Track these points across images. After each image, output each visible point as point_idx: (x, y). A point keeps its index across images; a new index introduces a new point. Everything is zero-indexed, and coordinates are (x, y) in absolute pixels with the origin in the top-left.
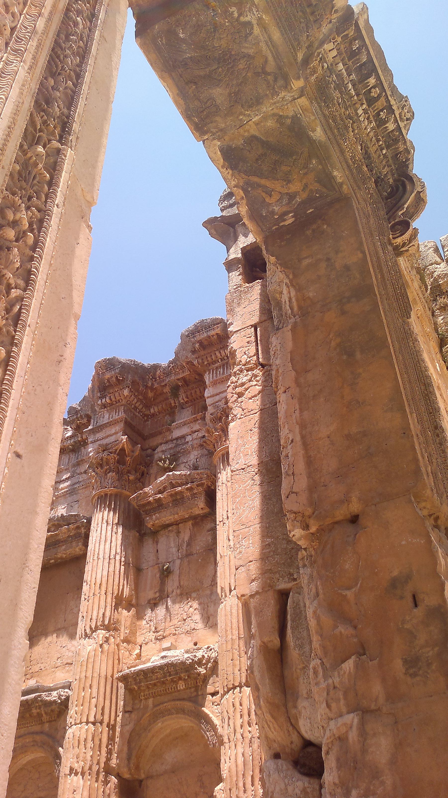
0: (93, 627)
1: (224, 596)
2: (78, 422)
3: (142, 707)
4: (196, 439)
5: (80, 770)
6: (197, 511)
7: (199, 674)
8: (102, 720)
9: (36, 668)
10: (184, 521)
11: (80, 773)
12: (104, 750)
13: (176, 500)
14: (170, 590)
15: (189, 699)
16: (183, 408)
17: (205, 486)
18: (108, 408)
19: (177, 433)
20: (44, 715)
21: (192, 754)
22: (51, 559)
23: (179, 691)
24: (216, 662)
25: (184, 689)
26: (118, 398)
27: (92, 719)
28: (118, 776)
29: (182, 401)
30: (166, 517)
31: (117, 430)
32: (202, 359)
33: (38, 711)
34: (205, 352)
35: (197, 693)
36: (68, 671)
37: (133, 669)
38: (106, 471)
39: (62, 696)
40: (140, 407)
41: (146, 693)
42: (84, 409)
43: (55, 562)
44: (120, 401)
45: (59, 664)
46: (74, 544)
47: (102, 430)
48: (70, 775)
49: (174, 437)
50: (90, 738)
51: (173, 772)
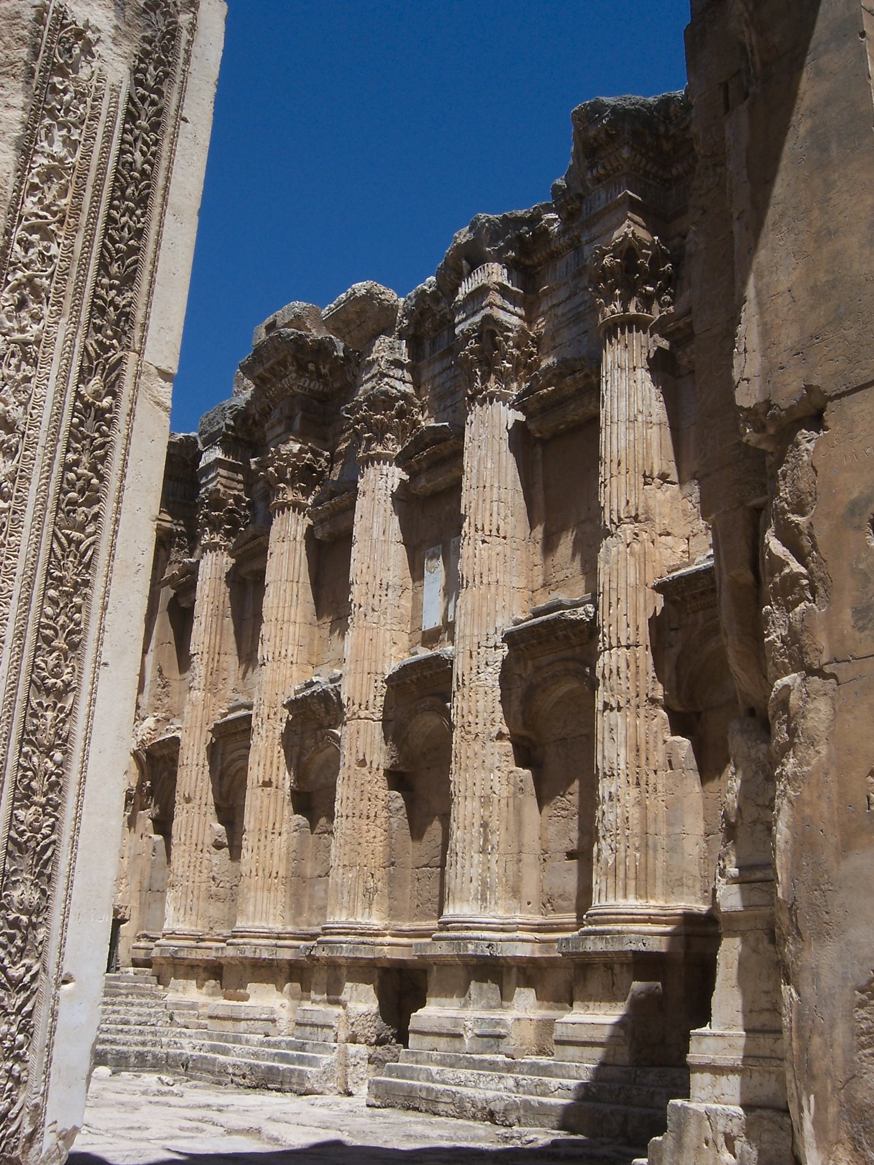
9: (560, 576)
20: (573, 637)
22: (560, 424)
28: (666, 708)
33: (565, 632)
37: (675, 574)
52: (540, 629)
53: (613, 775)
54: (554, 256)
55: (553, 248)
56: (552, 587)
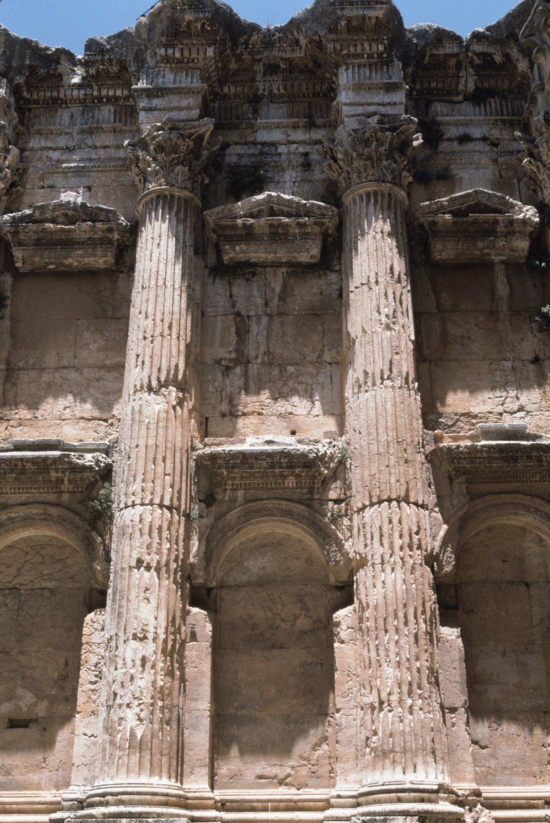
0: (163, 379)
1: (370, 384)
2: (101, 67)
3: (227, 498)
4: (294, 153)
5: (154, 564)
6: (303, 258)
7: (320, 474)
8: (180, 505)
10: (276, 265)
11: (153, 569)
12: (181, 544)
13: (276, 234)
14: (252, 354)
15: (300, 502)
16: (271, 102)
17: (325, 227)
18: (174, 65)
19: (263, 136)
21: (288, 569)
22: (52, 263)
23: (284, 488)
24: (342, 462)
25: (293, 488)
26: (194, 55)
27: (167, 502)
29: (276, 91)
30: (256, 253)
31: (191, 104)
32: (341, 46)
33: (60, 475)
34: (350, 37)
35: (312, 495)
36: (83, 429)
38: (172, 161)
39: (101, 462)
40: (214, 79)
41: (235, 482)
42: (116, 50)
43: (57, 268)
44: (196, 61)
46: (99, 252)
47: (163, 96)
48: (138, 567)
49: (259, 140)
50: (165, 526)
51: (261, 586)
52: (29, 465)
53: (145, 638)
54: (57, 103)
55: (62, 96)
56: (12, 423)
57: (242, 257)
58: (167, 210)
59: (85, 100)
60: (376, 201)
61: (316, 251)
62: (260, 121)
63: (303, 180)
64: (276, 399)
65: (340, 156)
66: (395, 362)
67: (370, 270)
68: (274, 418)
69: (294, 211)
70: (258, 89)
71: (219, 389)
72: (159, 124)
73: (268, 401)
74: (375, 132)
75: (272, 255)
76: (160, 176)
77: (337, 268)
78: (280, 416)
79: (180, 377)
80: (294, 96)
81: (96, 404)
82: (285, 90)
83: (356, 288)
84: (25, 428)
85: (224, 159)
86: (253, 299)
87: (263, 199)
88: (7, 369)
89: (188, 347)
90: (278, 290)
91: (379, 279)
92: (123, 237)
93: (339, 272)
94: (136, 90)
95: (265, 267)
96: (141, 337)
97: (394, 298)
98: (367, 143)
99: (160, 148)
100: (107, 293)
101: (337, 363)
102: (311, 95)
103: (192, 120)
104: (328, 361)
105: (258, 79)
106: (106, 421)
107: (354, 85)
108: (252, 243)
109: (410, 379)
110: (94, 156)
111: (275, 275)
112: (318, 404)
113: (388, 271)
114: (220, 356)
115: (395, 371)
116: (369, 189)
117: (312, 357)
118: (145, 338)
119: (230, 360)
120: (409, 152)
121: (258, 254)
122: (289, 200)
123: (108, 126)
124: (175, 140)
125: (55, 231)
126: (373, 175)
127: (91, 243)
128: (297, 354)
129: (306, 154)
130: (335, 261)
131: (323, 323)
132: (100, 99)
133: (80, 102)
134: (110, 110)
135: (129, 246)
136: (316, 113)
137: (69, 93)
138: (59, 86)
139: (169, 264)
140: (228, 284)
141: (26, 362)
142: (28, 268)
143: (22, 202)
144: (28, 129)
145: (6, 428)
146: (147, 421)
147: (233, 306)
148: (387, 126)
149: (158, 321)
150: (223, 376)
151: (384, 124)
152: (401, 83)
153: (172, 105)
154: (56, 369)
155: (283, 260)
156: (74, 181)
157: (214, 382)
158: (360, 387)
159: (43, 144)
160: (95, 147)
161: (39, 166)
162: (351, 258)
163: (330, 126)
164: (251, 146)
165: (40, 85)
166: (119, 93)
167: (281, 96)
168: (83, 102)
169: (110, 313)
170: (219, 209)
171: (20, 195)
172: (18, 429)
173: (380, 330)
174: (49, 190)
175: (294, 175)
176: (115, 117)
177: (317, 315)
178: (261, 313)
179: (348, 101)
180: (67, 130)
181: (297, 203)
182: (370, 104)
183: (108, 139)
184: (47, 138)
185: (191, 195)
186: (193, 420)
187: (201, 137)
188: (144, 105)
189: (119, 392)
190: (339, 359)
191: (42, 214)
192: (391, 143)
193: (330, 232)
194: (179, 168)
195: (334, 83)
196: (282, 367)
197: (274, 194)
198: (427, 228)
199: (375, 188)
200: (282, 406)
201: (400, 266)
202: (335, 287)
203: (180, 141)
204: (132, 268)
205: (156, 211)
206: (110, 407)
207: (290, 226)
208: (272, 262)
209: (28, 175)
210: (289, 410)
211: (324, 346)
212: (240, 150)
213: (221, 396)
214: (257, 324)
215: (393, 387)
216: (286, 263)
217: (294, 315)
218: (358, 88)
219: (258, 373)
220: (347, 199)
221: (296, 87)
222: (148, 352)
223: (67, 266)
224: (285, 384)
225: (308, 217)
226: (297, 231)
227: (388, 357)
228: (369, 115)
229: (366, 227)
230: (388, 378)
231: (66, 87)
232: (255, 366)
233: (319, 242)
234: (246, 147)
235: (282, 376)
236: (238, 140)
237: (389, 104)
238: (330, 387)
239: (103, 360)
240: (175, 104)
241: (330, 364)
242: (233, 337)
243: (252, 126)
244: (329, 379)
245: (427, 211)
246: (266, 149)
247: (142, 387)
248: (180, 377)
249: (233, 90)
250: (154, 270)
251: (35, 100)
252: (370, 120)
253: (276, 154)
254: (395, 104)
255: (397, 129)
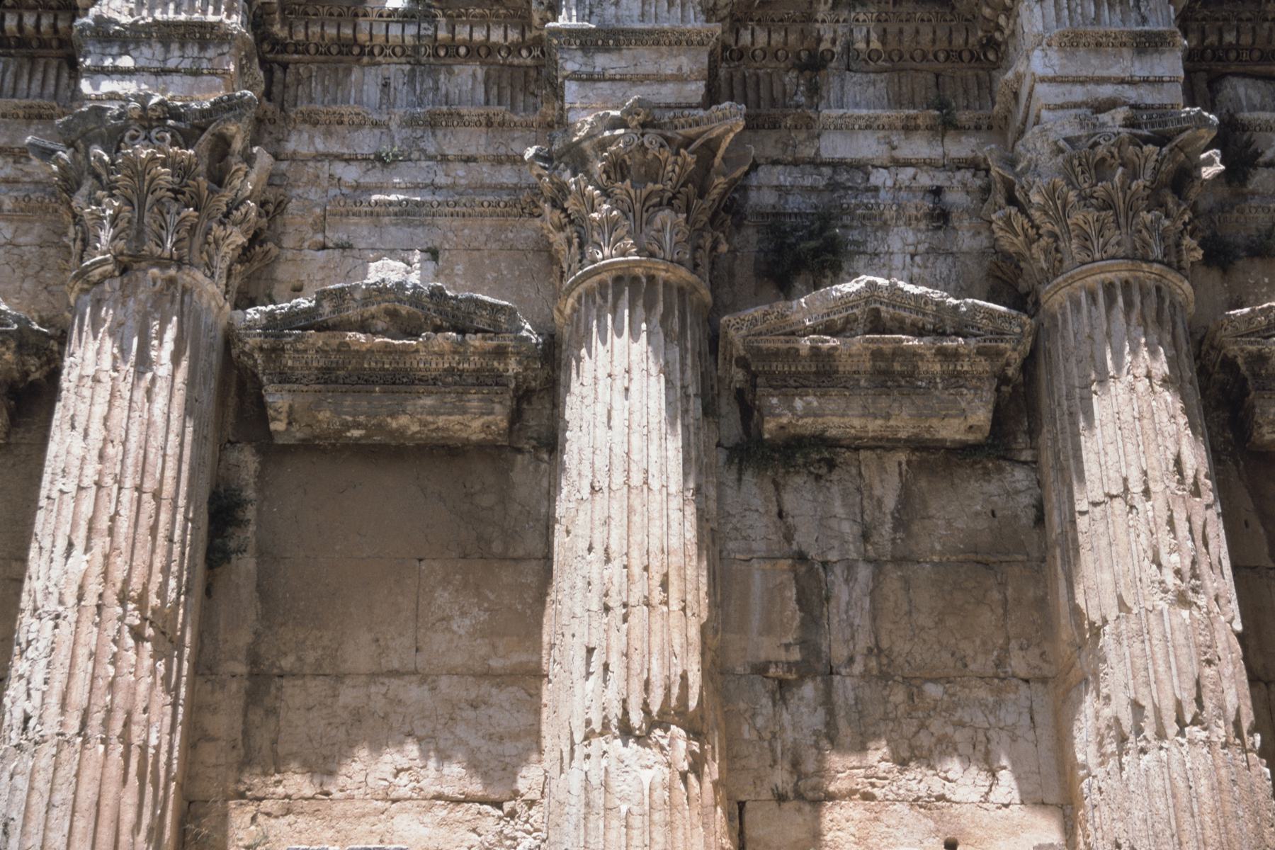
0: (655, 708)
1: (1149, 732)
4: (909, 188)
6: (951, 430)
10: (883, 445)
13: (888, 373)
14: (839, 652)
16: (849, 70)
17: (1002, 361)
19: (834, 146)
22: (358, 425)
29: (861, 45)
30: (842, 417)
36: (443, 823)
38: (647, 199)
43: (366, 437)
45: (402, 792)
46: (474, 402)
47: (618, 47)
49: (826, 155)
54: (351, 52)
55: (363, 37)
56: (267, 805)
57: (808, 425)
58: (640, 311)
59: (416, 49)
60: (1129, 304)
61: (981, 416)
62: (830, 113)
63: (933, 251)
64: (903, 763)
65: (1036, 198)
66: (1207, 683)
67: (1128, 465)
68: (902, 808)
69: (929, 323)
70: (819, 40)
71: (767, 735)
72: (617, 113)
73: (884, 765)
74: (1119, 145)
75: (879, 422)
76: (621, 232)
77: (1026, 455)
78: (916, 802)
79: (693, 703)
80: (901, 58)
81: (474, 766)
82: (884, 43)
83: (1095, 504)
84: (301, 819)
85: (745, 198)
86: (833, 523)
87: (858, 293)
88: (251, 675)
89: (703, 629)
90: (890, 503)
91: (1151, 485)
92: (526, 369)
93: (1034, 465)
94: (556, 32)
95: (857, 449)
96: (595, 605)
97: (1191, 531)
98: (1100, 169)
99: (618, 169)
100: (487, 500)
101: (1044, 680)
102: (942, 56)
103: (690, 107)
104: (1022, 674)
105: (820, 16)
106: (498, 805)
107: (1063, 35)
108: (834, 392)
109: (1246, 725)
110: (441, 180)
111: (882, 469)
112: (1006, 777)
113: (1171, 468)
114: (763, 656)
115: (1209, 705)
116: (1110, 276)
117: (981, 663)
118: (607, 609)
119: (790, 666)
120: (1192, 195)
121: (846, 420)
122: (916, 297)
123: (475, 111)
124: (653, 151)
125: (370, 351)
126: (1118, 244)
127: (454, 382)
128: (946, 656)
129: (937, 192)
130: (1022, 440)
131: (1002, 585)
132: (452, 48)
133: (403, 53)
134: (474, 76)
135: (533, 391)
136: (955, 97)
137: (379, 31)
138: (356, 15)
139: (654, 436)
140: (771, 487)
141: (299, 659)
142: (299, 433)
143: (275, 280)
144: (282, 109)
145: (254, 819)
146: (624, 808)
147: (788, 537)
148: (1145, 132)
149: (636, 570)
150: (774, 705)
151: (1139, 127)
152: (1173, 34)
153: (640, 70)
154: (373, 676)
155: (903, 435)
156: (397, 234)
157: (754, 715)
158: (1123, 739)
159: (320, 145)
160: (444, 159)
161: (312, 196)
162: (1076, 435)
163: (990, 128)
164: (808, 168)
165: (311, 10)
166: (497, 36)
167: (872, 56)
168: (411, 54)
169: (497, 547)
170: (757, 312)
171: (270, 263)
172: (283, 821)
173: (1163, 605)
174: (337, 253)
175: (911, 238)
176: (486, 92)
177: (986, 565)
178: (853, 555)
179: (1050, 73)
180: (375, 117)
181: (937, 304)
182: (1100, 81)
183: (474, 141)
184: (328, 134)
185: (692, 278)
186: (719, 809)
187: (710, 147)
188: (576, 67)
189: (532, 739)
190: (1047, 670)
191: (337, 309)
192: (1156, 171)
193: (1010, 372)
194: (665, 216)
195: (999, 28)
196: (913, 686)
197: (881, 281)
198: (1243, 368)
199: (1125, 274)
200: (919, 781)
201: (1195, 459)
202: (1025, 500)
203: (666, 153)
204: (551, 443)
205: (615, 310)
206: (509, 771)
207: (922, 356)
208: (873, 438)
209: (287, 217)
210: (938, 790)
211: (1008, 639)
212: (782, 176)
213: (773, 750)
214: (847, 581)
215: (1208, 743)
216: (907, 440)
217: (932, 561)
218: (1071, 42)
219: (857, 700)
220: (1055, 297)
221: (907, 39)
222: (617, 643)
223: (392, 433)
224: (922, 726)
225: (965, 337)
226: (937, 368)
227: (1192, 669)
228: (1101, 107)
229: (1110, 363)
230: (1195, 721)
231: (374, 17)
232: (848, 681)
233: (989, 395)
234: (796, 172)
235: (916, 709)
236: (775, 153)
237: (1146, 81)
238: (1030, 736)
239: (485, 659)
240: (648, 67)
241: (1027, 681)
242: (792, 613)
243: (808, 124)
244: (1026, 719)
245: (1243, 328)
246: (843, 177)
247: (606, 726)
248: (693, 703)
249: (762, 38)
250: (619, 450)
251: (297, 44)
252: (1104, 117)
253: (867, 190)
254: (1160, 81)
255: (1170, 140)
